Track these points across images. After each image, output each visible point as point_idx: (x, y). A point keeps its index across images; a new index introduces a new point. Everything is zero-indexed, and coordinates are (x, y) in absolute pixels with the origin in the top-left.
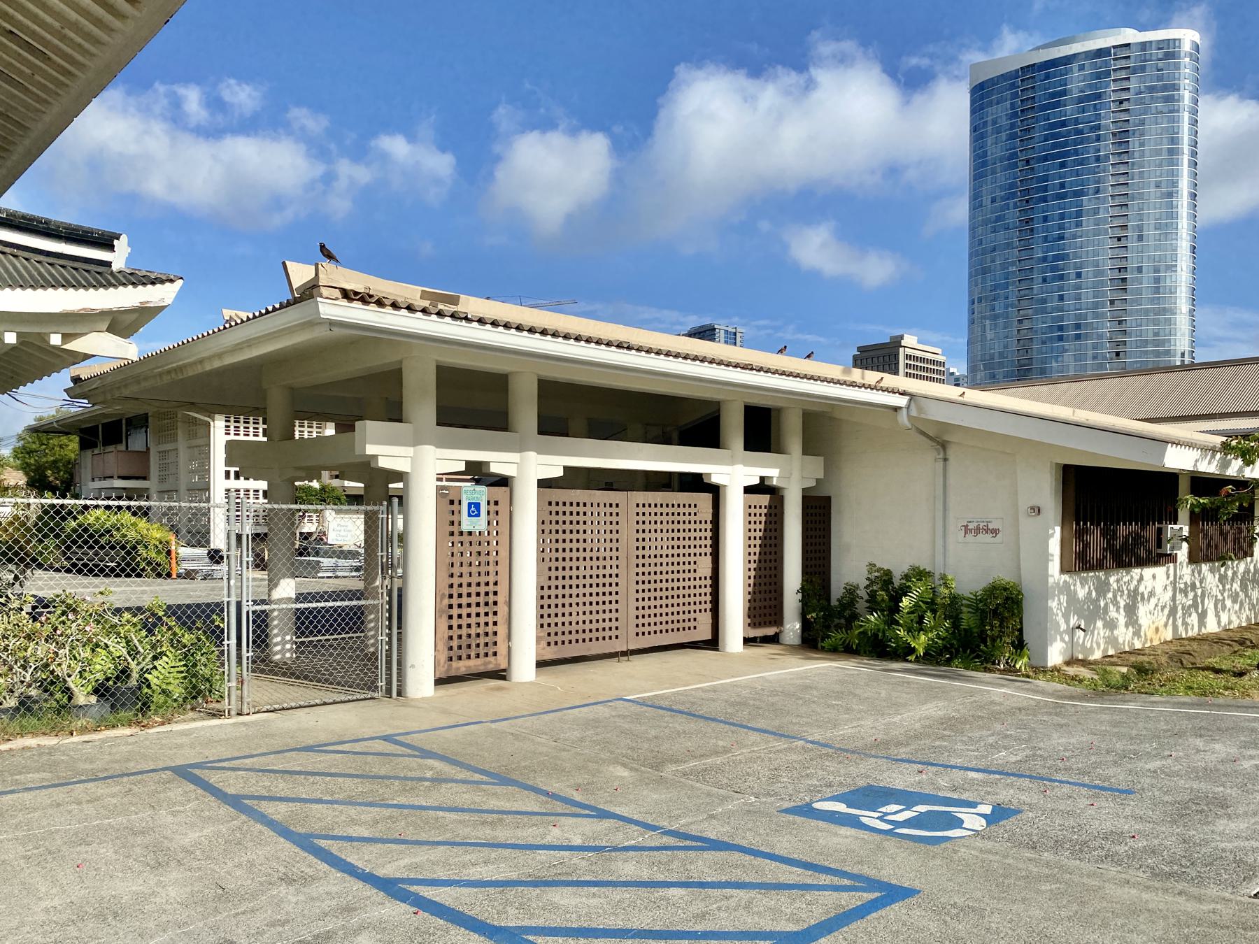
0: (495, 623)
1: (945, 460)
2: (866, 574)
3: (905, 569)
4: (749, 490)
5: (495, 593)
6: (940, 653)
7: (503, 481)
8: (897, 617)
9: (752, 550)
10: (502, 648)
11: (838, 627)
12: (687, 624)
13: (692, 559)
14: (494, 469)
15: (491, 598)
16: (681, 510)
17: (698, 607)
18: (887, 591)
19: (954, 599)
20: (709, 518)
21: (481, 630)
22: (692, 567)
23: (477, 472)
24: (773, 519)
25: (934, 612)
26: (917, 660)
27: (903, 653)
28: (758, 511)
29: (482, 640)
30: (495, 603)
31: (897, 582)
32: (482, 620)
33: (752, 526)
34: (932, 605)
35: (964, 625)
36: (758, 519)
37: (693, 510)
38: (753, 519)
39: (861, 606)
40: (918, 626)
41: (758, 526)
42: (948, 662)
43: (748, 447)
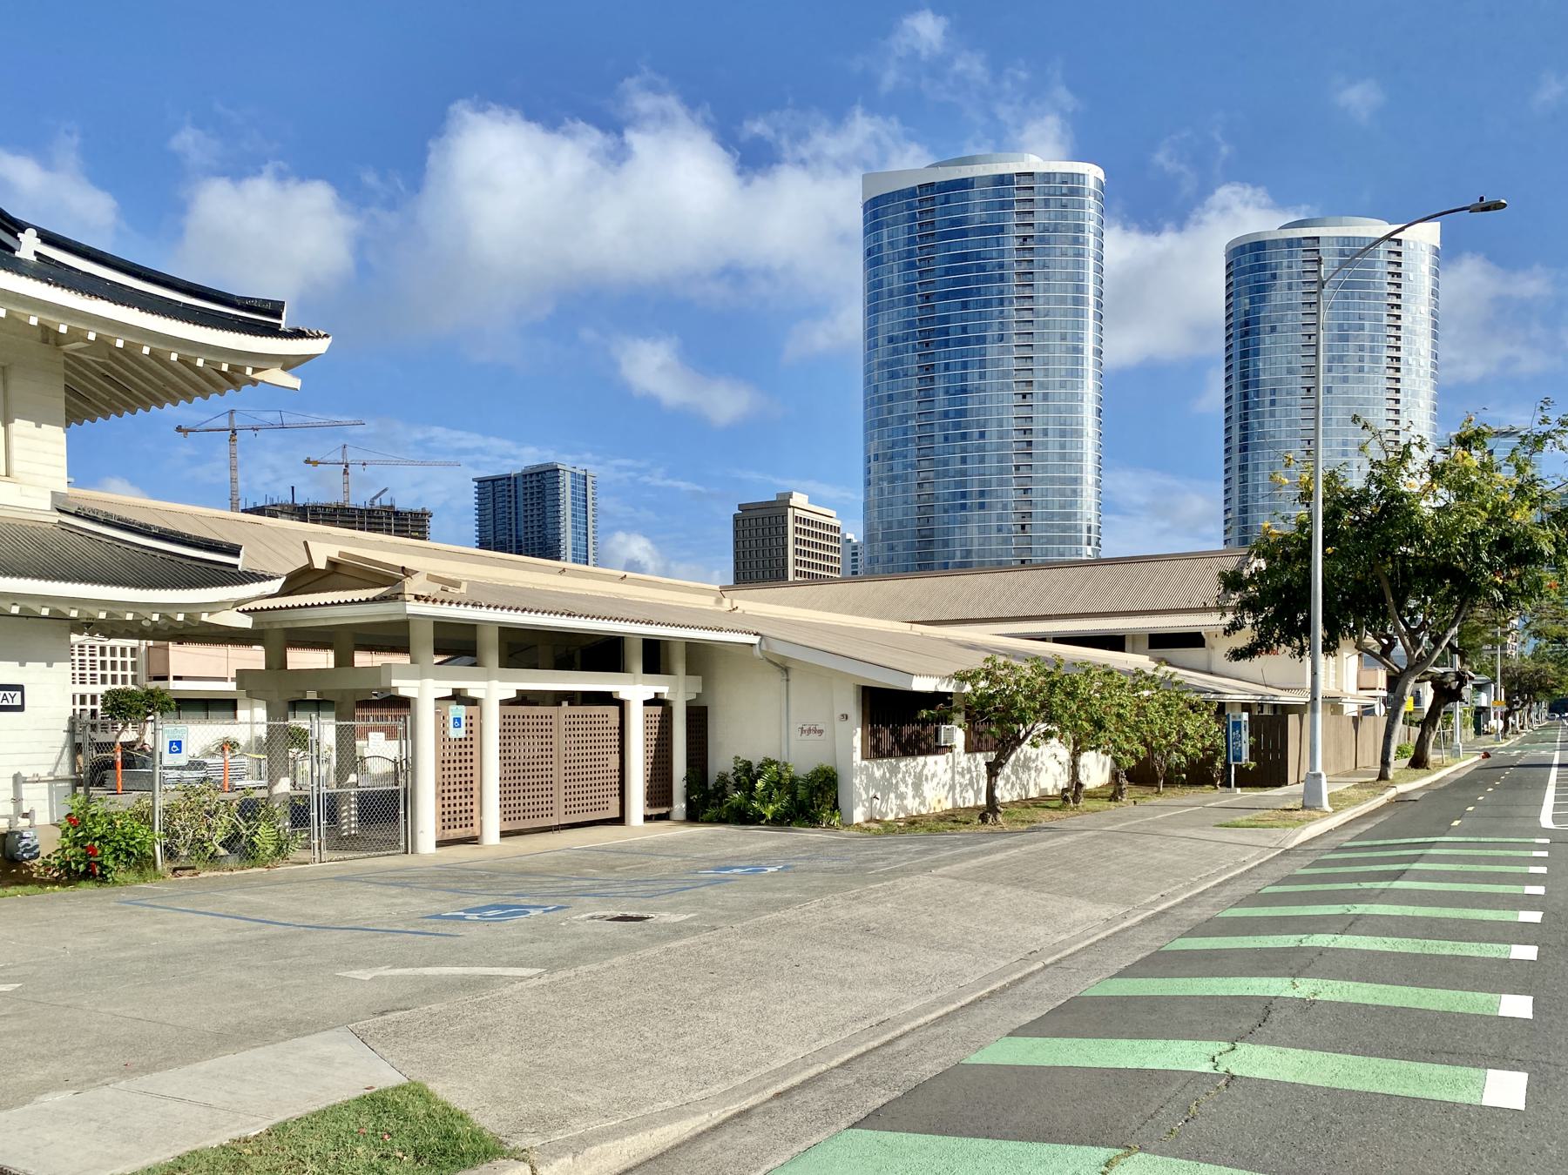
0: (472, 803)
1: (788, 680)
2: (733, 765)
3: (761, 760)
4: (646, 703)
5: (472, 782)
6: (783, 818)
7: (474, 702)
8: (754, 794)
9: (650, 748)
11: (714, 805)
12: (602, 806)
13: (605, 756)
14: (471, 694)
15: (469, 786)
16: (597, 719)
17: (609, 793)
18: (748, 776)
19: (793, 780)
20: (617, 725)
22: (605, 762)
23: (458, 697)
24: (665, 724)
25: (779, 789)
26: (767, 823)
27: (755, 819)
28: (653, 719)
30: (472, 789)
31: (755, 770)
33: (650, 731)
34: (778, 785)
35: (799, 798)
36: (653, 725)
37: (605, 719)
38: (650, 725)
39: (730, 787)
40: (768, 799)
41: (654, 731)
42: (789, 824)
43: (646, 670)
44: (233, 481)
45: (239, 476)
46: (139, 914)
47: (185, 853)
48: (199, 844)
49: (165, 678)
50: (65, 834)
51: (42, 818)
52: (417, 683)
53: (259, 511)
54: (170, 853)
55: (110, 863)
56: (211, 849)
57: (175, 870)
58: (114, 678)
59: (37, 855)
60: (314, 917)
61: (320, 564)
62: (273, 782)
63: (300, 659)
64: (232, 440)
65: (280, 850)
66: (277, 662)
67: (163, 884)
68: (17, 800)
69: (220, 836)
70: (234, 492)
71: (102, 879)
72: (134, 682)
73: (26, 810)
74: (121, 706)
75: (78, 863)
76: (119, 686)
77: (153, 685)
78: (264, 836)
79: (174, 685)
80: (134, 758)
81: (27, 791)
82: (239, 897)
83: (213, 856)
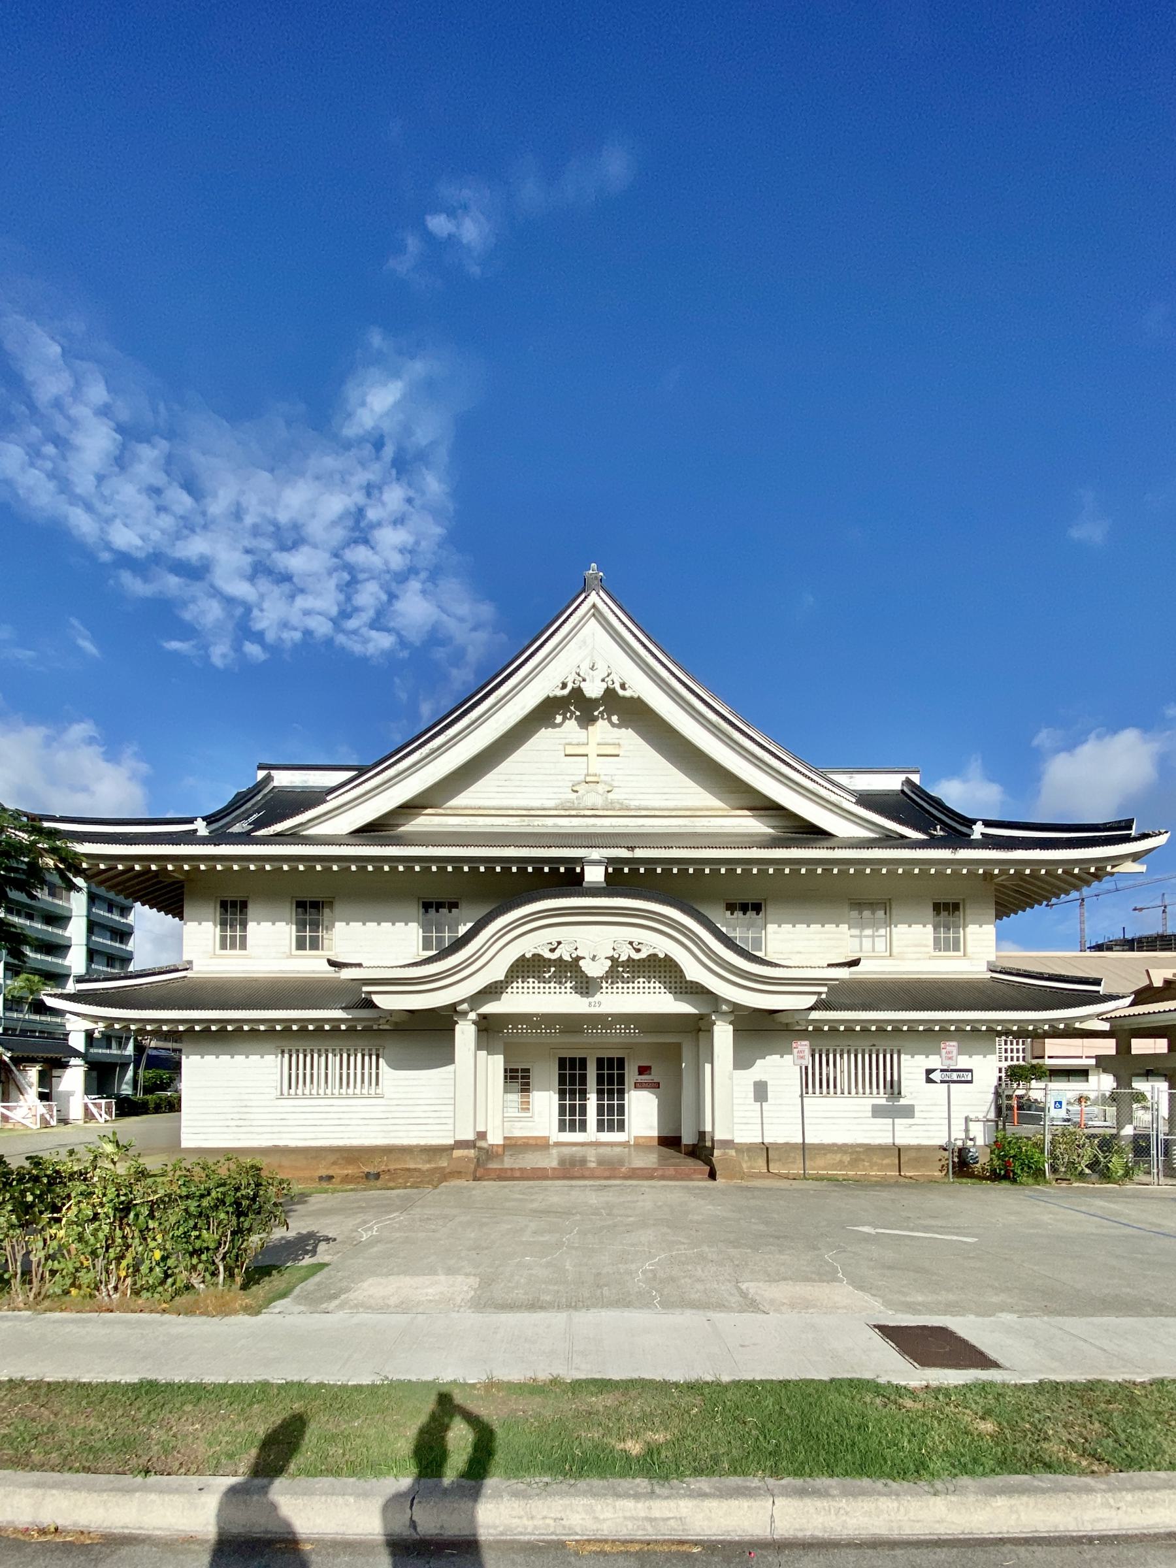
44: (1082, 930)
45: (1086, 926)
46: (1039, 1206)
47: (1063, 1170)
48: (1072, 1165)
49: (1043, 1057)
50: (992, 1152)
51: (980, 1141)
53: (1099, 948)
54: (1054, 1170)
55: (1019, 1172)
56: (1080, 1168)
57: (1057, 1180)
59: (977, 1162)
60: (1159, 1226)
62: (1120, 1126)
63: (1140, 1046)
64: (1081, 905)
65: (1128, 1173)
66: (1124, 1048)
67: (1052, 1189)
68: (967, 1130)
69: (1084, 1163)
70: (1082, 937)
71: (1014, 1181)
72: (1024, 1060)
73: (971, 1137)
74: (1016, 1074)
75: (1000, 1170)
76: (1015, 1063)
77: (1035, 1062)
78: (1116, 1163)
79: (1048, 1062)
80: (1025, 1105)
81: (972, 1125)
82: (1100, 1203)
83: (1082, 1173)
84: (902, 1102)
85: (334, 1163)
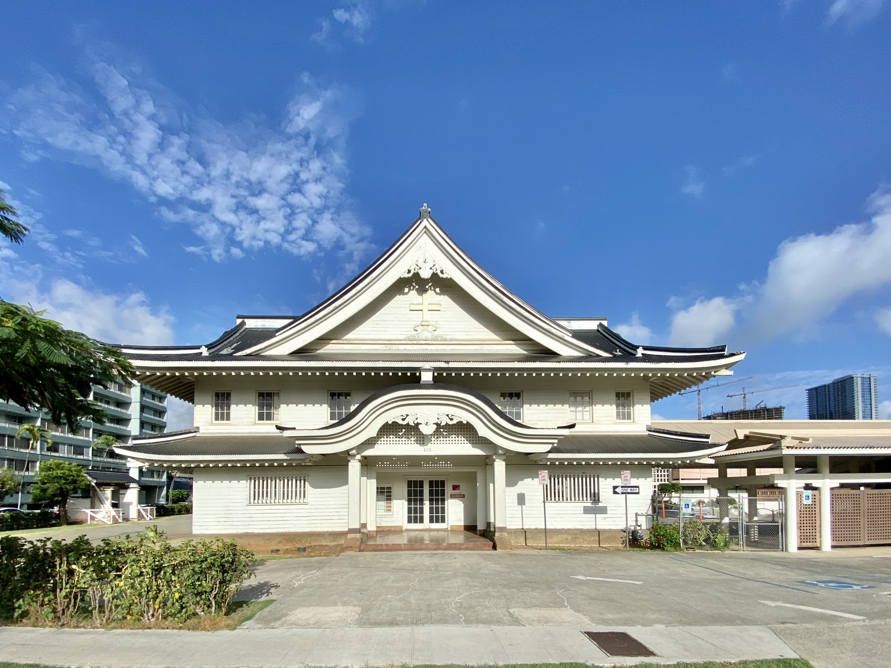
10: (818, 540)
15: (814, 525)
21: (811, 534)
29: (811, 537)
32: (811, 531)
44: (699, 408)
45: (702, 406)
46: (677, 563)
47: (690, 543)
48: (695, 540)
49: (679, 479)
50: (651, 533)
51: (644, 527)
52: (787, 481)
53: (709, 418)
54: (685, 543)
55: (666, 544)
56: (699, 542)
57: (687, 548)
58: (661, 480)
59: (642, 539)
60: (744, 574)
61: (741, 437)
62: (722, 518)
63: (732, 473)
64: (699, 394)
65: (726, 545)
66: (723, 474)
67: (683, 554)
68: (636, 521)
69: (702, 539)
70: (699, 412)
71: (663, 549)
72: (668, 481)
74: (664, 489)
75: (655, 543)
76: (663, 482)
77: (674, 482)
78: (720, 539)
79: (681, 482)
80: (669, 506)
82: (711, 561)
83: (701, 545)
84: (600, 505)
85: (280, 542)
